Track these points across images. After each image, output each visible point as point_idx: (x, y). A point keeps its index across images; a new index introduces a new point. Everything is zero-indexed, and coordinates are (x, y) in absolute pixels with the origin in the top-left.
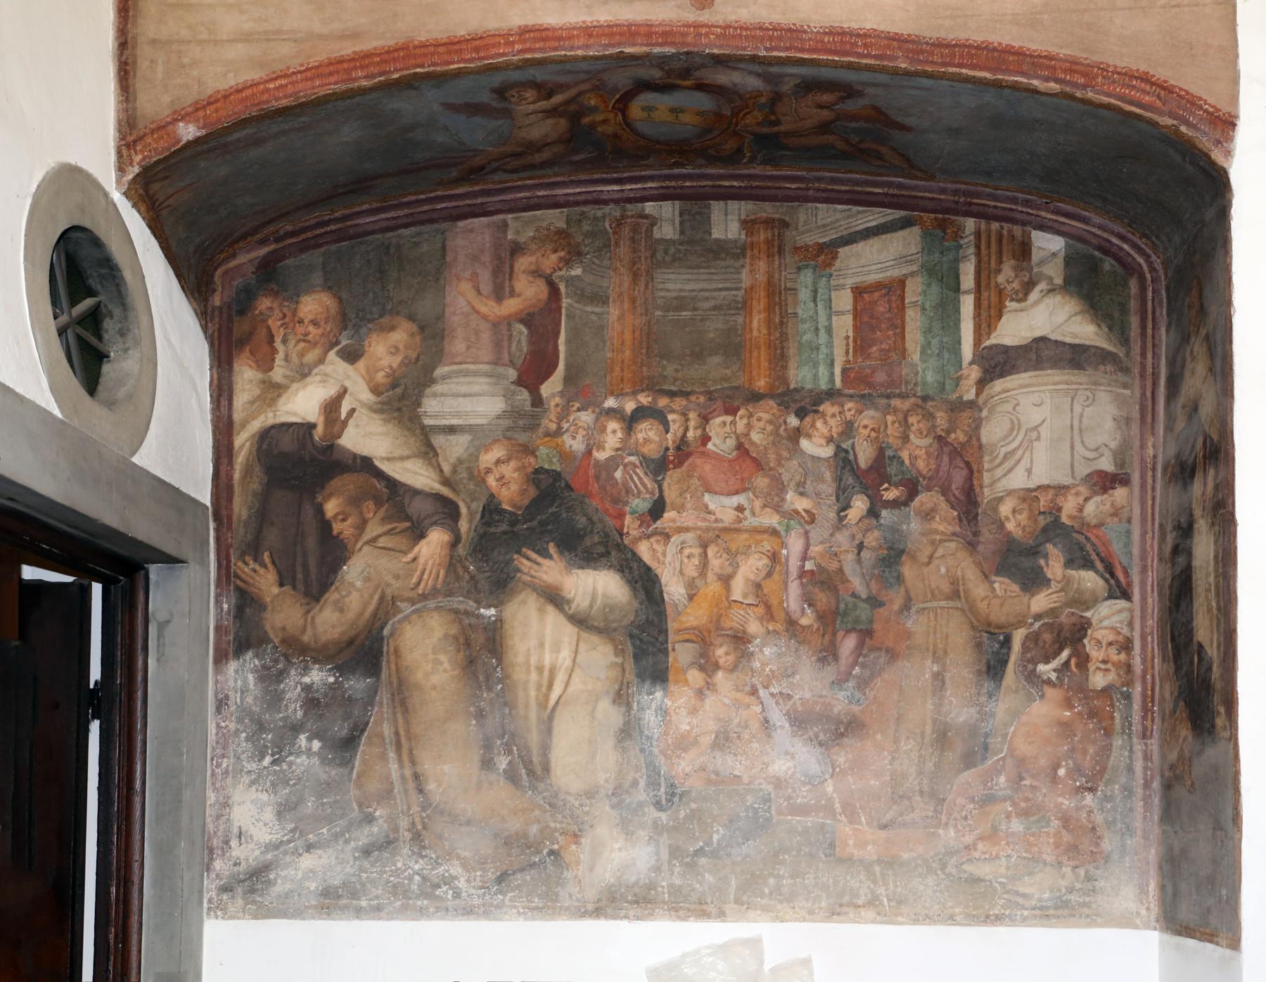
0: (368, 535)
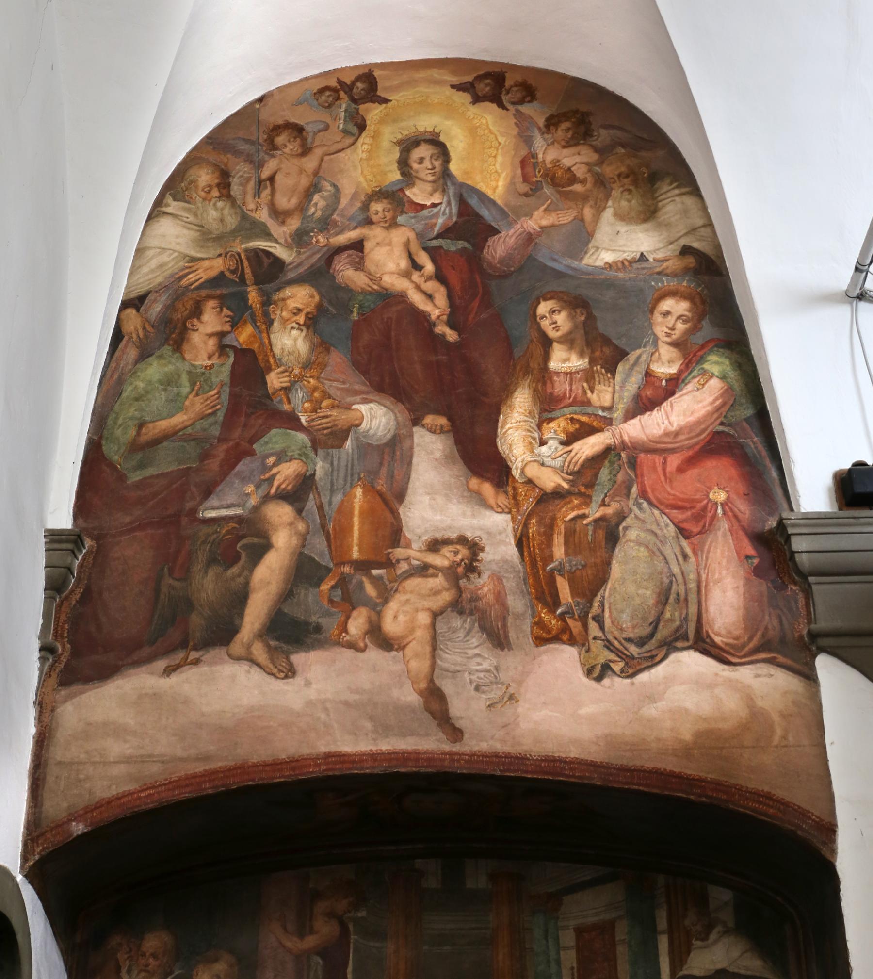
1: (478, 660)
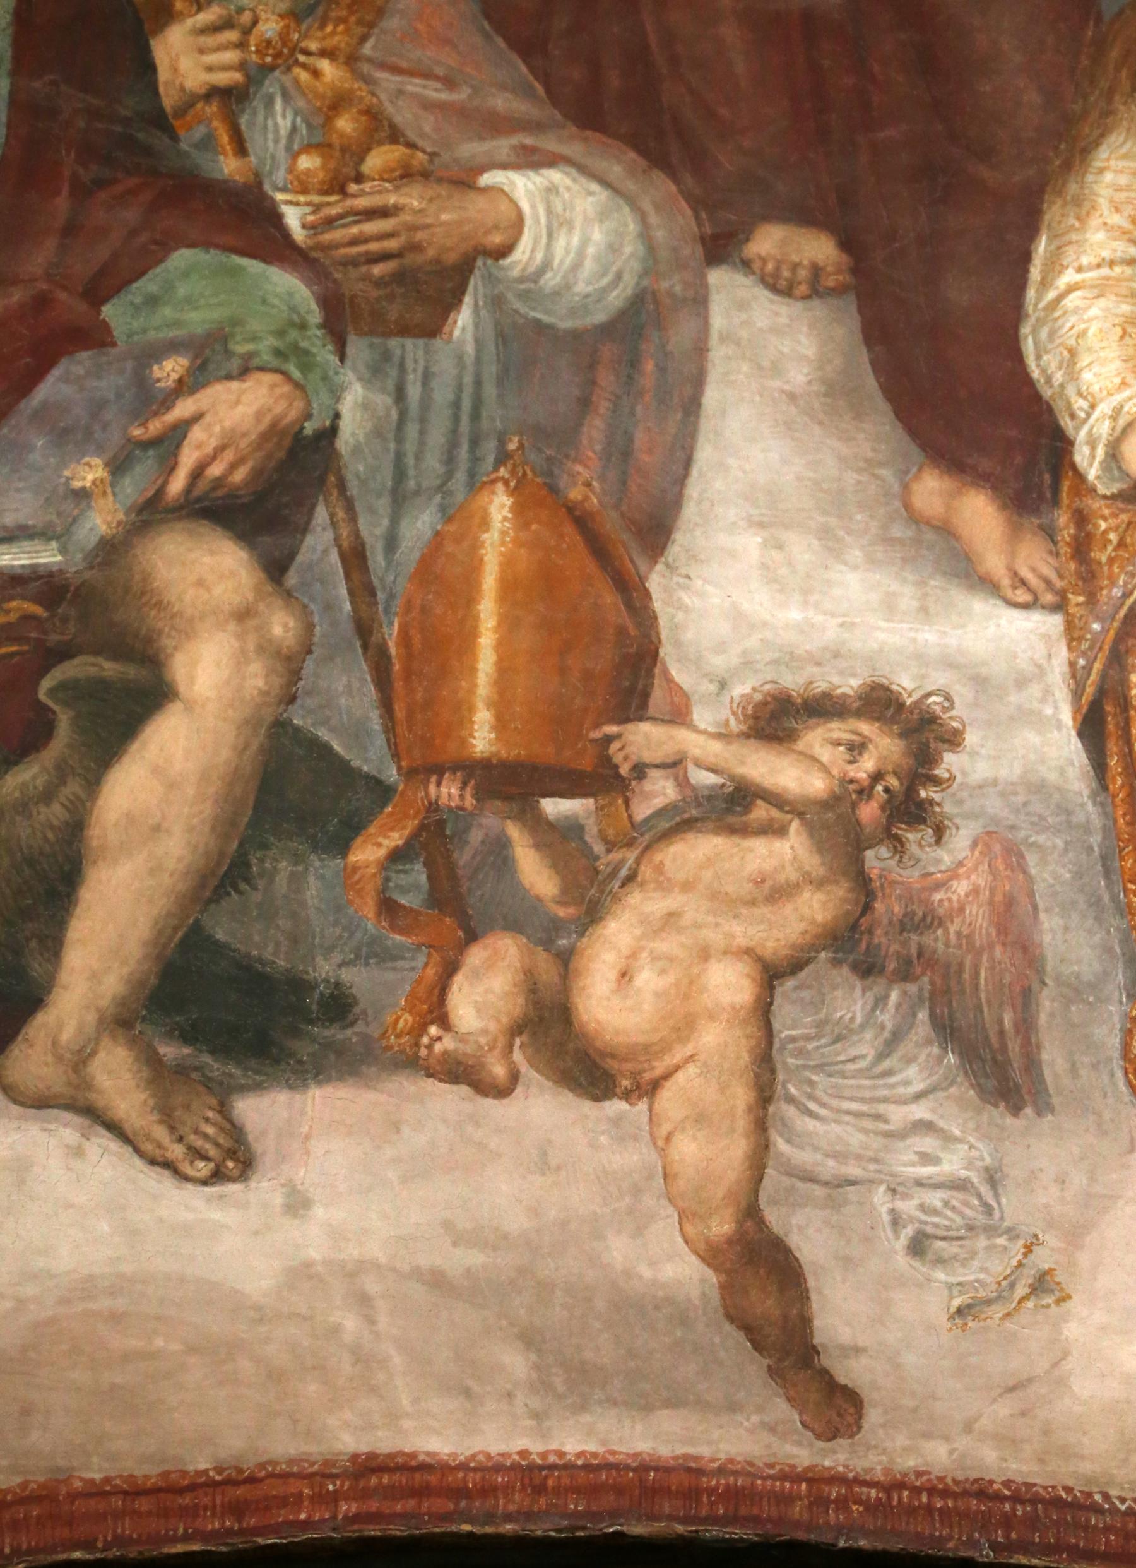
1: (927, 1143)
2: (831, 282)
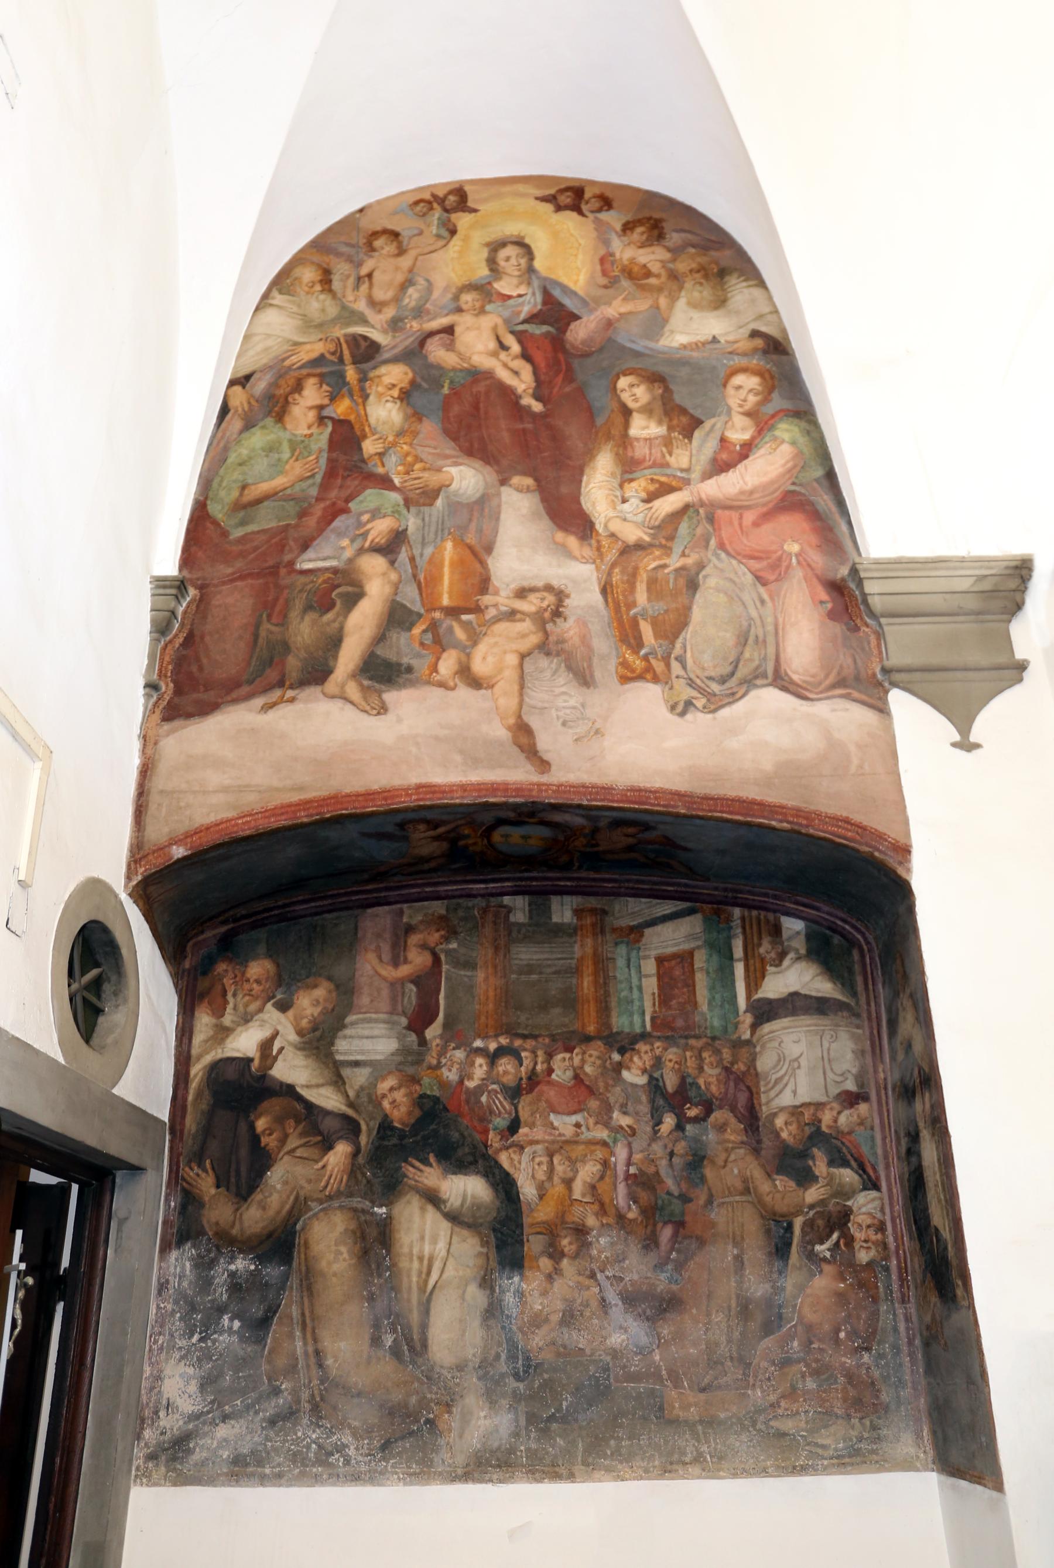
0: (287, 1148)
2: (532, 488)
